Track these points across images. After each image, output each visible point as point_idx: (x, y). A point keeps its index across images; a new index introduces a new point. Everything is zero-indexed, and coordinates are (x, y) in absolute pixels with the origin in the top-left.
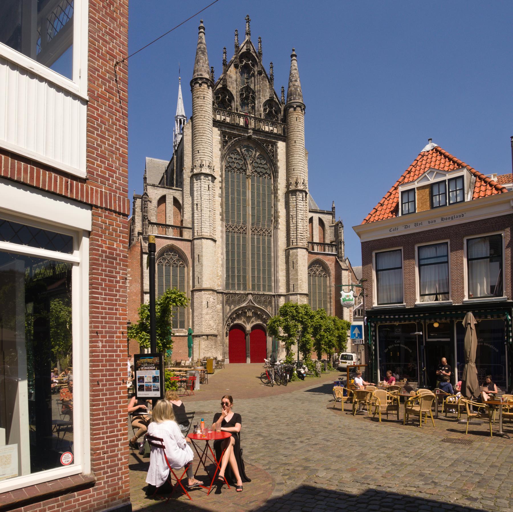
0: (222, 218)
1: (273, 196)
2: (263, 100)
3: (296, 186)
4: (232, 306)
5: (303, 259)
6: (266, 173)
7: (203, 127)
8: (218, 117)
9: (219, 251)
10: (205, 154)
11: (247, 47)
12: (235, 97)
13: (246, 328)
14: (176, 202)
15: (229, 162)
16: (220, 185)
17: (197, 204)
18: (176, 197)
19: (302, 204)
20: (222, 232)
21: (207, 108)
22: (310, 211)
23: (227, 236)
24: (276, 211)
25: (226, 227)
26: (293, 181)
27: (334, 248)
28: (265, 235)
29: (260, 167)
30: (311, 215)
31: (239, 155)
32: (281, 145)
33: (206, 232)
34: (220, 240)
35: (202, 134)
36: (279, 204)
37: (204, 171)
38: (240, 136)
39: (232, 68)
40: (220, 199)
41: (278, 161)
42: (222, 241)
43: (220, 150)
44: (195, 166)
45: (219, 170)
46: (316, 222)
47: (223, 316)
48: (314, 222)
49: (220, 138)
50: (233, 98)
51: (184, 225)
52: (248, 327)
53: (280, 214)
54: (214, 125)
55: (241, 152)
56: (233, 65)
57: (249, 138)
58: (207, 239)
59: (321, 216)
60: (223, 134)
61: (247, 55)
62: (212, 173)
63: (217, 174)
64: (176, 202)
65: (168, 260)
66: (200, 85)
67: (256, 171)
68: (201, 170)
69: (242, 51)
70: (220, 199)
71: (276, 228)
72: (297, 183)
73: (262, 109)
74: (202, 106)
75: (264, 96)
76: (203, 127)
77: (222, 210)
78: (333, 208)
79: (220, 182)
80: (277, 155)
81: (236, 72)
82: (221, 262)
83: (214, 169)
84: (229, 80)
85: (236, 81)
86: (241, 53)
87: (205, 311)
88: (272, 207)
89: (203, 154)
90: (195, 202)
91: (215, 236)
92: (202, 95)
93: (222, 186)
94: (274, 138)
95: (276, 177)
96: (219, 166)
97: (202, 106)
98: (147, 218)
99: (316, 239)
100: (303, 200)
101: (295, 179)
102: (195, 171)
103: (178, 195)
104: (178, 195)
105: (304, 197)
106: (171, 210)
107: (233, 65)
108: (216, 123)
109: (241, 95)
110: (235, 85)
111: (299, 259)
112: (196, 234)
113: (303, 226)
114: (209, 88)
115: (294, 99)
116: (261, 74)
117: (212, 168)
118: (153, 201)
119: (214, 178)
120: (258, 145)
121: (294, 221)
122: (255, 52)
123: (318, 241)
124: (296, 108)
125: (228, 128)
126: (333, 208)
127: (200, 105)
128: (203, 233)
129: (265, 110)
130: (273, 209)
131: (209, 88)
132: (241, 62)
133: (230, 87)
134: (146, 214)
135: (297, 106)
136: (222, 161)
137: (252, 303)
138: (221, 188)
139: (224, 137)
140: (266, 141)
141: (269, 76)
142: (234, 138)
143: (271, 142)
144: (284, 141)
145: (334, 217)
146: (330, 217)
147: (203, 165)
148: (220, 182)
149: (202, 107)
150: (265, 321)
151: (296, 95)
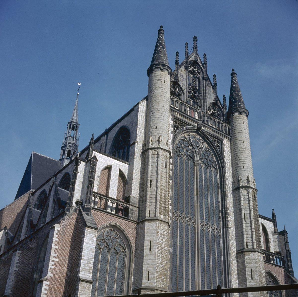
1: (219, 190)
12: (185, 92)
14: (121, 174)
18: (122, 170)
39: (183, 68)
50: (183, 93)
56: (183, 67)
61: (195, 63)
64: (121, 174)
69: (191, 59)
84: (180, 77)
88: (219, 202)
107: (183, 67)
122: (202, 63)
126: (274, 216)
130: (220, 204)
141: (213, 84)
145: (275, 226)
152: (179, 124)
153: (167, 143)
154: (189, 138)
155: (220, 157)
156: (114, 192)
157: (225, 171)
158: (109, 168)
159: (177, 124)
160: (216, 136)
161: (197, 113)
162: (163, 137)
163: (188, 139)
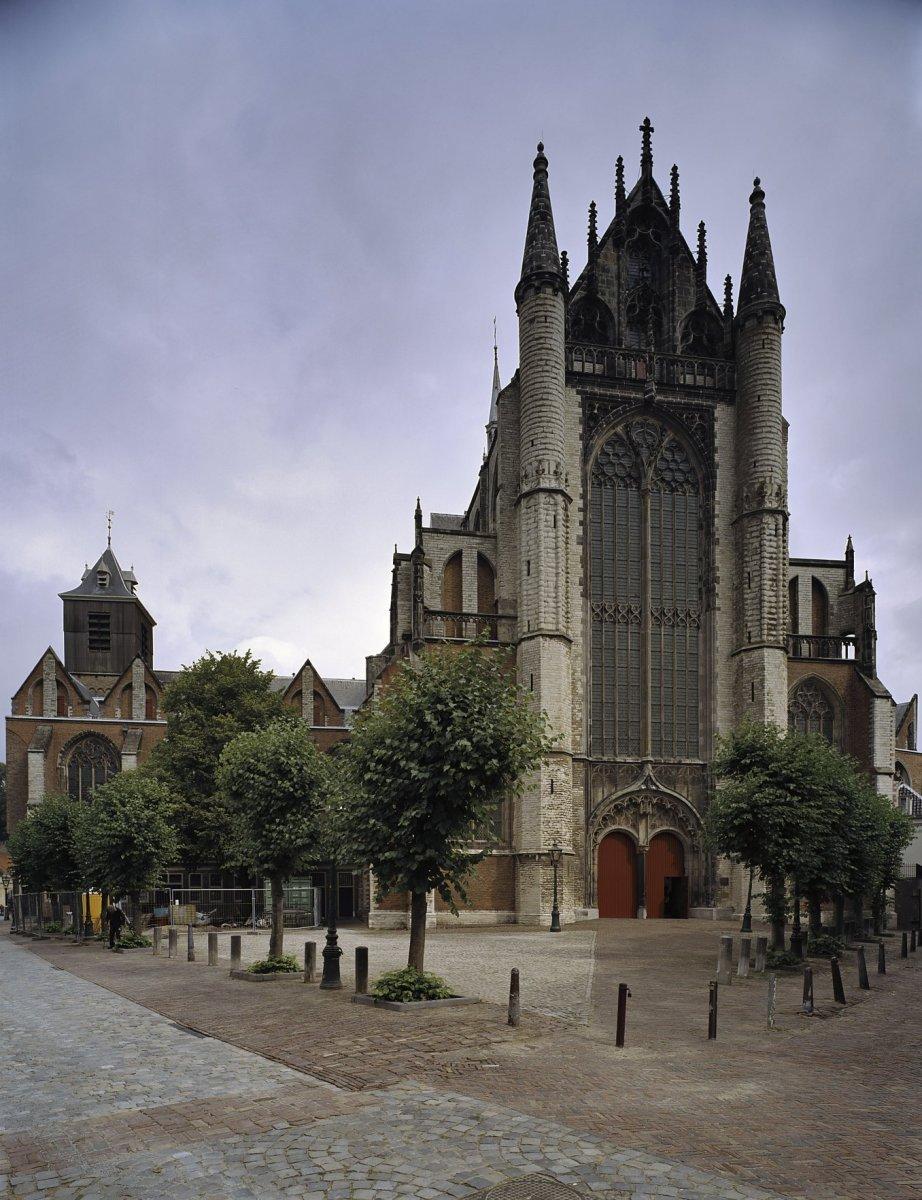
0: (585, 590)
2: (682, 314)
3: (761, 502)
5: (776, 677)
6: (687, 481)
7: (543, 385)
8: (577, 367)
9: (579, 665)
10: (550, 447)
11: (644, 194)
12: (616, 315)
16: (580, 516)
19: (774, 544)
20: (584, 621)
21: (552, 342)
22: (791, 564)
23: (597, 632)
24: (710, 568)
25: (593, 611)
27: (852, 649)
28: (685, 627)
29: (671, 470)
30: (792, 572)
32: (722, 414)
33: (548, 626)
34: (580, 640)
35: (541, 403)
36: (718, 549)
37: (542, 485)
38: (627, 400)
40: (581, 547)
41: (715, 450)
42: (585, 642)
43: (581, 437)
45: (579, 482)
47: (586, 813)
48: (800, 588)
49: (580, 410)
51: (500, 612)
52: (643, 835)
53: (718, 574)
54: (568, 382)
55: (629, 438)
57: (649, 402)
58: (551, 637)
59: (818, 572)
60: (587, 402)
62: (563, 487)
63: (575, 489)
66: (538, 290)
67: (663, 480)
68: (539, 483)
69: (634, 205)
70: (581, 547)
71: (710, 608)
73: (678, 335)
74: (541, 338)
75: (685, 305)
76: (543, 385)
77: (585, 573)
78: (850, 553)
79: (580, 510)
80: (713, 436)
81: (619, 258)
82: (580, 691)
83: (566, 481)
85: (618, 277)
86: (629, 210)
87: (546, 801)
89: (543, 446)
91: (570, 632)
93: (585, 519)
94: (708, 397)
95: (710, 488)
96: (579, 473)
97: (541, 338)
98: (422, 602)
99: (806, 628)
100: (775, 536)
101: (757, 486)
102: (525, 488)
104: (486, 547)
105: (781, 526)
106: (471, 584)
108: (572, 378)
109: (631, 308)
110: (615, 289)
111: (767, 677)
113: (773, 597)
115: (757, 298)
116: (678, 254)
117: (563, 477)
119: (568, 499)
120: (667, 416)
121: (752, 585)
123: (809, 632)
124: (761, 317)
125: (600, 385)
126: (850, 553)
127: (536, 336)
128: (543, 626)
129: (685, 337)
132: (630, 233)
133: (603, 294)
134: (420, 593)
135: (766, 312)
136: (585, 461)
138: (581, 523)
140: (687, 407)
142: (613, 408)
143: (698, 408)
144: (730, 402)
146: (840, 573)
148: (580, 510)
149: (542, 341)
150: (682, 823)
151: (763, 287)
157: (714, 484)
159: (596, 411)
160: (696, 405)
163: (625, 438)
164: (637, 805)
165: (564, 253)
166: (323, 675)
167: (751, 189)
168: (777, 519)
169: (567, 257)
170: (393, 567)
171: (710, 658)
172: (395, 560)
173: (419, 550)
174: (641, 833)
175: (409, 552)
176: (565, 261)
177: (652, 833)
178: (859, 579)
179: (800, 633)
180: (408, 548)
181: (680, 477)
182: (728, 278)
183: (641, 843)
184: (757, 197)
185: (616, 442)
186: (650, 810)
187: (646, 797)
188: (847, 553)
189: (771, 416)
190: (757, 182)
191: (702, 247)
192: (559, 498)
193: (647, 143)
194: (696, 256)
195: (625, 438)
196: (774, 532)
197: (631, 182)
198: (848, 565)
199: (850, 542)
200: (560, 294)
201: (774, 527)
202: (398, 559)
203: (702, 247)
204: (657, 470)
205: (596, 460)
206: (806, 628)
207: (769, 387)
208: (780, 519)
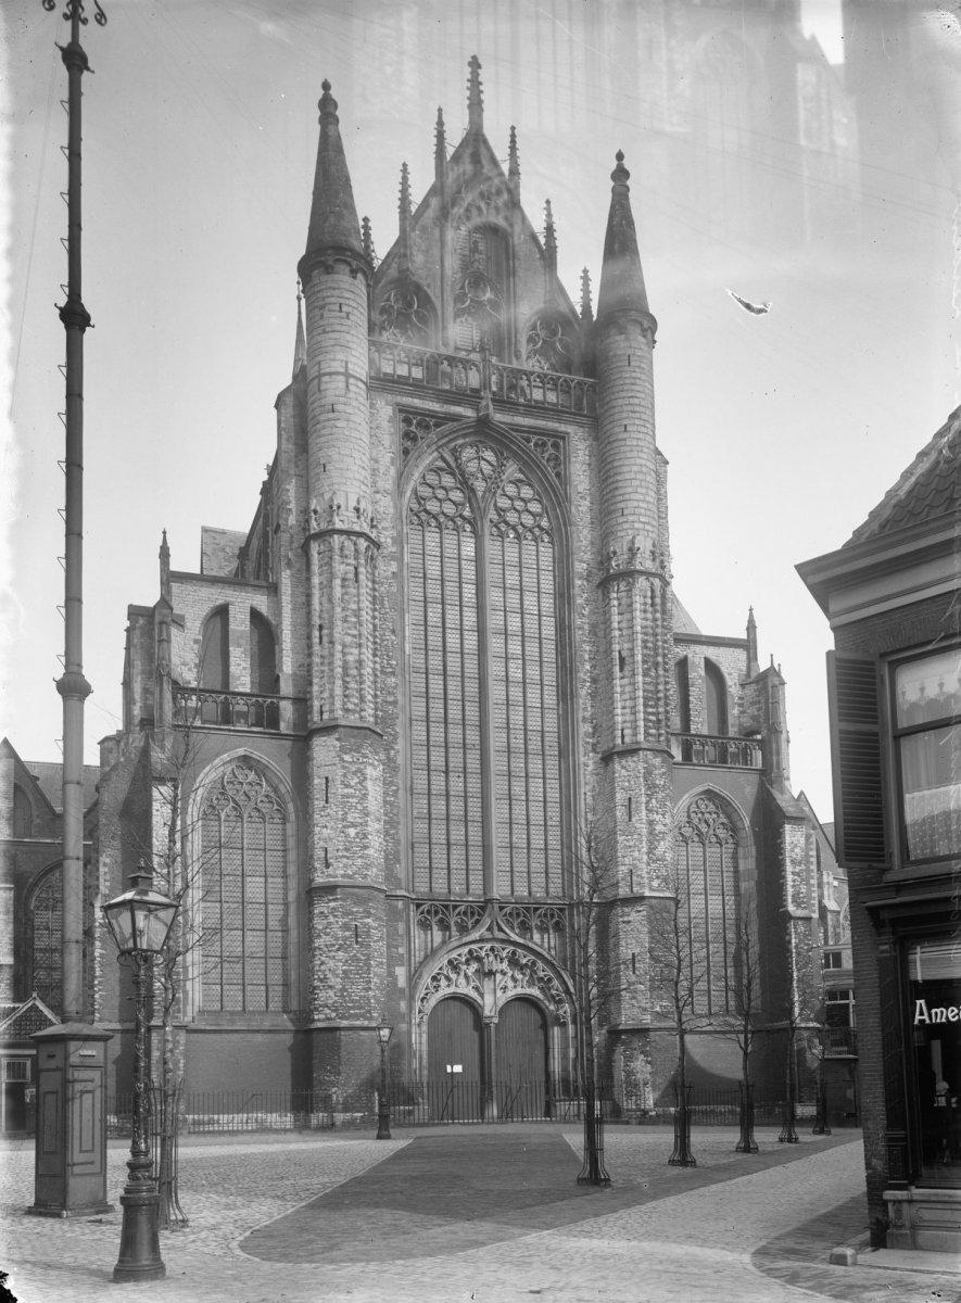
4: (438, 936)
12: (438, 305)
13: (483, 1008)
14: (255, 615)
15: (419, 499)
17: (321, 627)
26: (620, 546)
30: (680, 651)
31: (453, 474)
44: (315, 512)
46: (697, 674)
52: (490, 1004)
60: (406, 415)
62: (366, 529)
64: (255, 615)
65: (234, 801)
66: (329, 270)
72: (633, 551)
78: (751, 627)
90: (316, 621)
92: (333, 300)
98: (169, 674)
99: (701, 724)
102: (314, 527)
103: (261, 602)
104: (261, 602)
108: (381, 383)
112: (316, 718)
114: (355, 278)
118: (188, 624)
123: (705, 731)
126: (751, 627)
131: (355, 278)
137: (500, 929)
139: (407, 421)
141: (542, 240)
142: (437, 425)
146: (741, 655)
147: (339, 507)
152: (419, 424)
153: (357, 510)
154: (456, 460)
155: (555, 495)
156: (242, 676)
158: (222, 612)
159: (413, 428)
161: (478, 371)
162: (343, 494)
163: (453, 465)
164: (479, 959)
165: (366, 220)
166: (24, 757)
167: (614, 164)
168: (652, 584)
169: (370, 224)
170: (128, 624)
171: (574, 761)
172: (129, 614)
173: (165, 602)
174: (486, 996)
175: (151, 604)
176: (367, 228)
177: (502, 998)
178: (763, 664)
179: (693, 732)
180: (150, 597)
181: (528, 520)
182: (585, 271)
183: (487, 1012)
184: (621, 175)
185: (442, 469)
186: (496, 966)
187: (492, 949)
188: (748, 629)
189: (641, 451)
190: (620, 156)
191: (550, 229)
192: (363, 543)
193: (475, 84)
194: (542, 240)
195: (453, 465)
196: (649, 601)
197: (455, 137)
198: (748, 645)
199: (751, 615)
200: (360, 276)
201: (649, 594)
202: (135, 612)
203: (550, 229)
204: (499, 510)
205: (415, 492)
206: (701, 724)
207: (638, 415)
208: (657, 582)
